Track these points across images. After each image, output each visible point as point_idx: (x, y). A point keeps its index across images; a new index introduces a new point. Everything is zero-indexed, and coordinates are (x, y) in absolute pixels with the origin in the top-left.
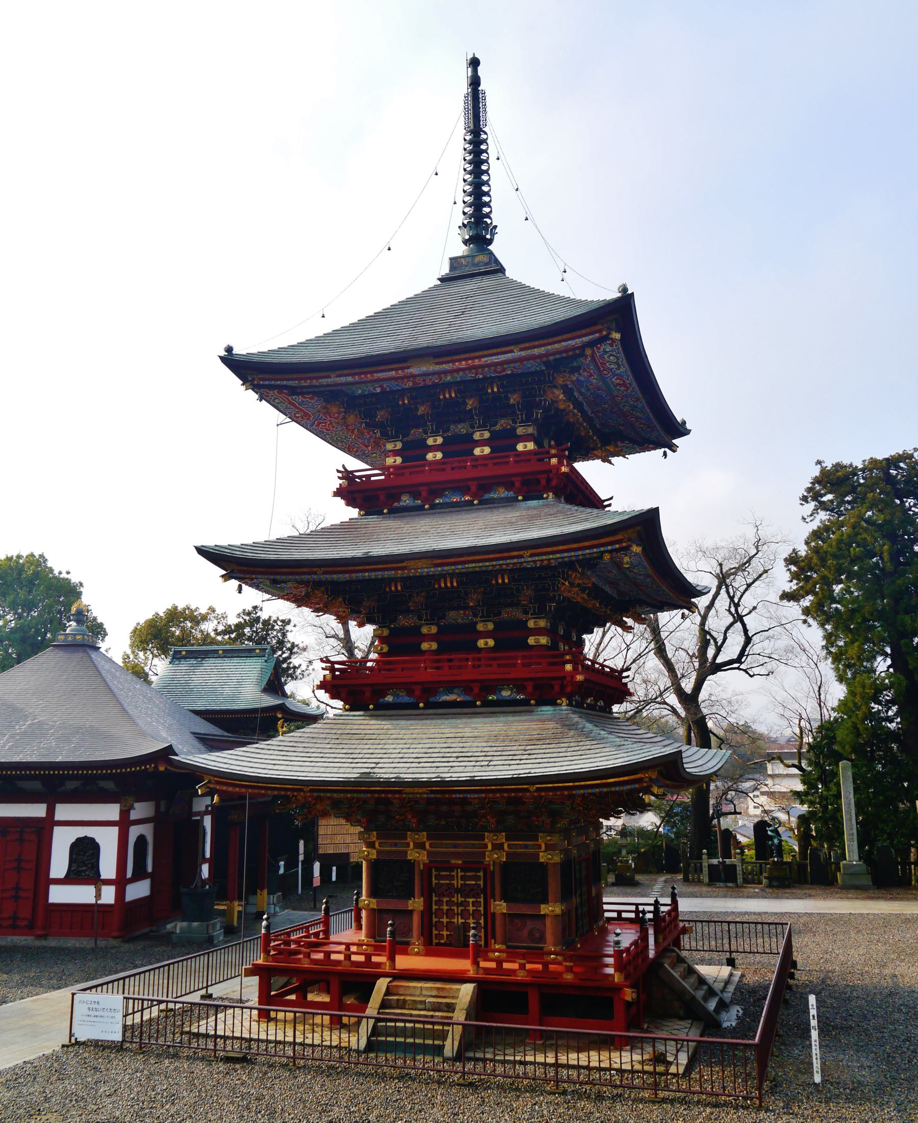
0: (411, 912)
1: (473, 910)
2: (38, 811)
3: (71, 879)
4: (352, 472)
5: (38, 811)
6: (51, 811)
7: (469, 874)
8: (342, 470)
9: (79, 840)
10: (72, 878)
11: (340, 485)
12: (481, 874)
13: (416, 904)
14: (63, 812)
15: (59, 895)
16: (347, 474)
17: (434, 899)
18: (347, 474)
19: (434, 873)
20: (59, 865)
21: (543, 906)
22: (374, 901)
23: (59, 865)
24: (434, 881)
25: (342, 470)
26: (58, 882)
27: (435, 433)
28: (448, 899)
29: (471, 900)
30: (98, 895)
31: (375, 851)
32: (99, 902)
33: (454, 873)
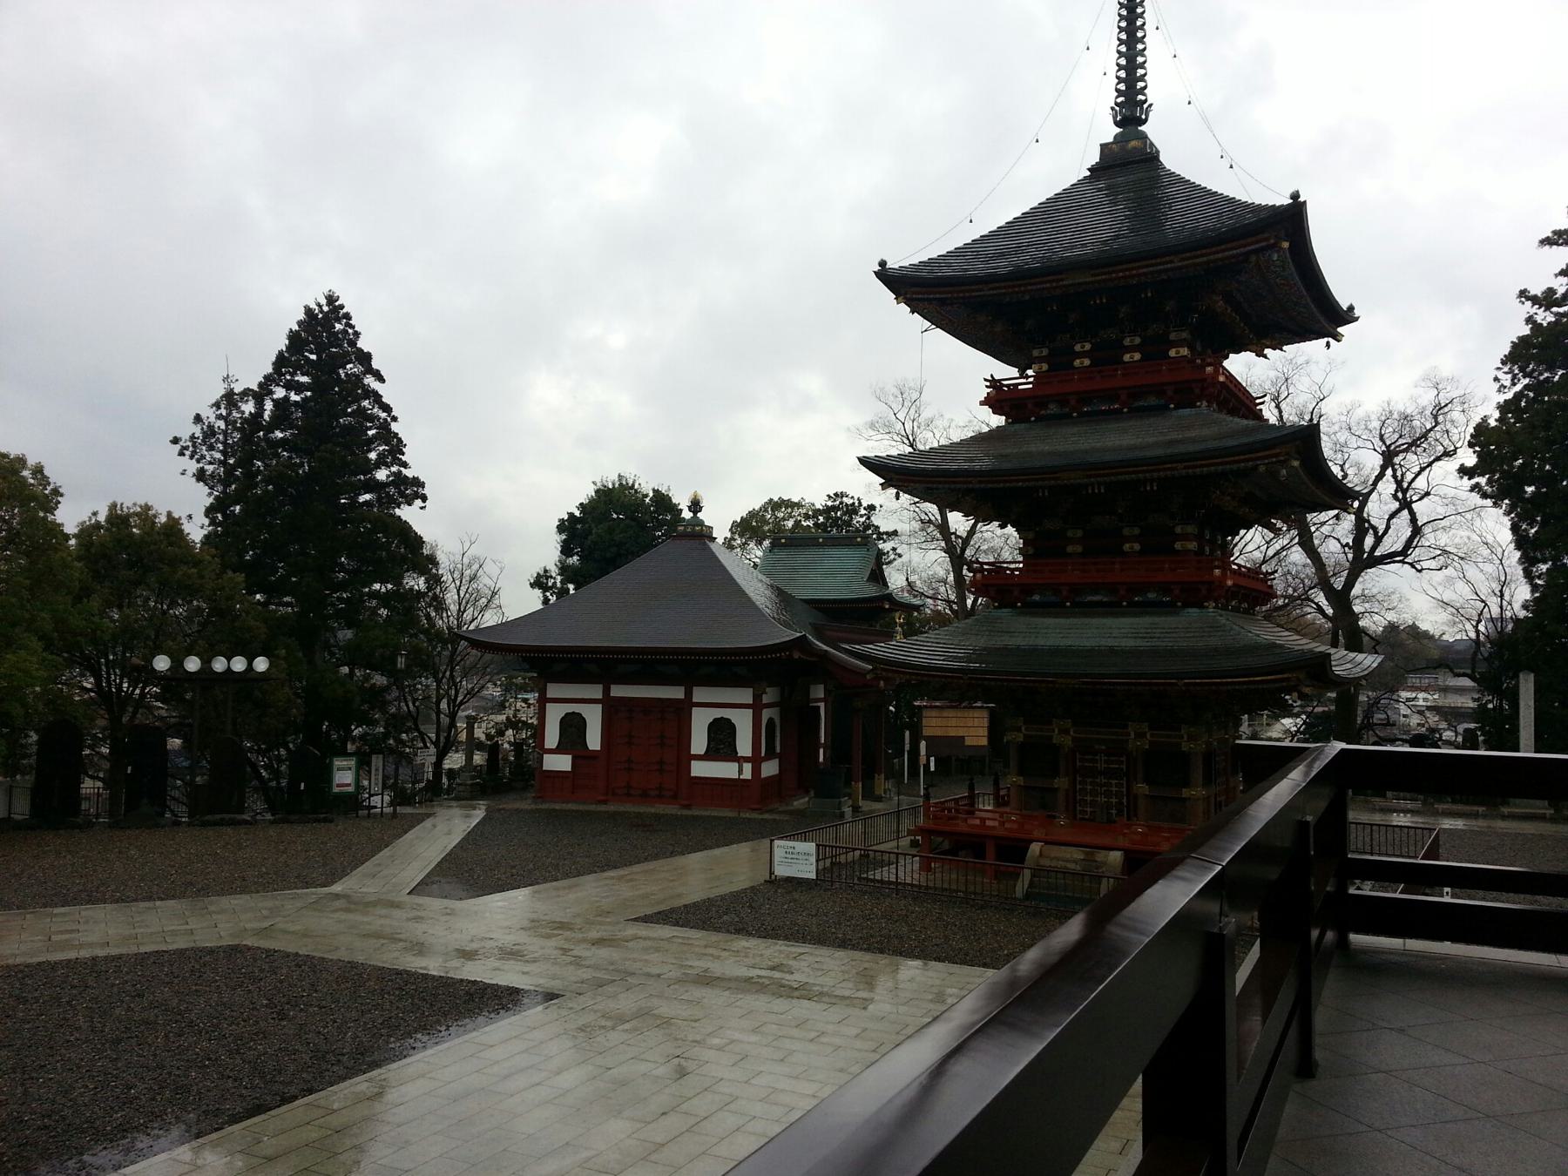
0: (1056, 790)
1: (1112, 791)
2: (677, 693)
3: (709, 756)
4: (1000, 381)
5: (677, 693)
6: (689, 694)
7: (1113, 758)
8: (990, 378)
9: (716, 720)
10: (711, 755)
11: (988, 393)
12: (1124, 759)
13: (1061, 783)
14: (700, 695)
15: (700, 769)
16: (994, 383)
17: (1078, 779)
18: (994, 383)
19: (1078, 756)
20: (699, 743)
21: (1184, 790)
22: (1021, 778)
23: (699, 743)
24: (1078, 764)
25: (990, 378)
26: (699, 758)
27: (1083, 340)
28: (1091, 780)
29: (1114, 782)
30: (741, 771)
31: (1022, 735)
32: (741, 777)
33: (1098, 757)
